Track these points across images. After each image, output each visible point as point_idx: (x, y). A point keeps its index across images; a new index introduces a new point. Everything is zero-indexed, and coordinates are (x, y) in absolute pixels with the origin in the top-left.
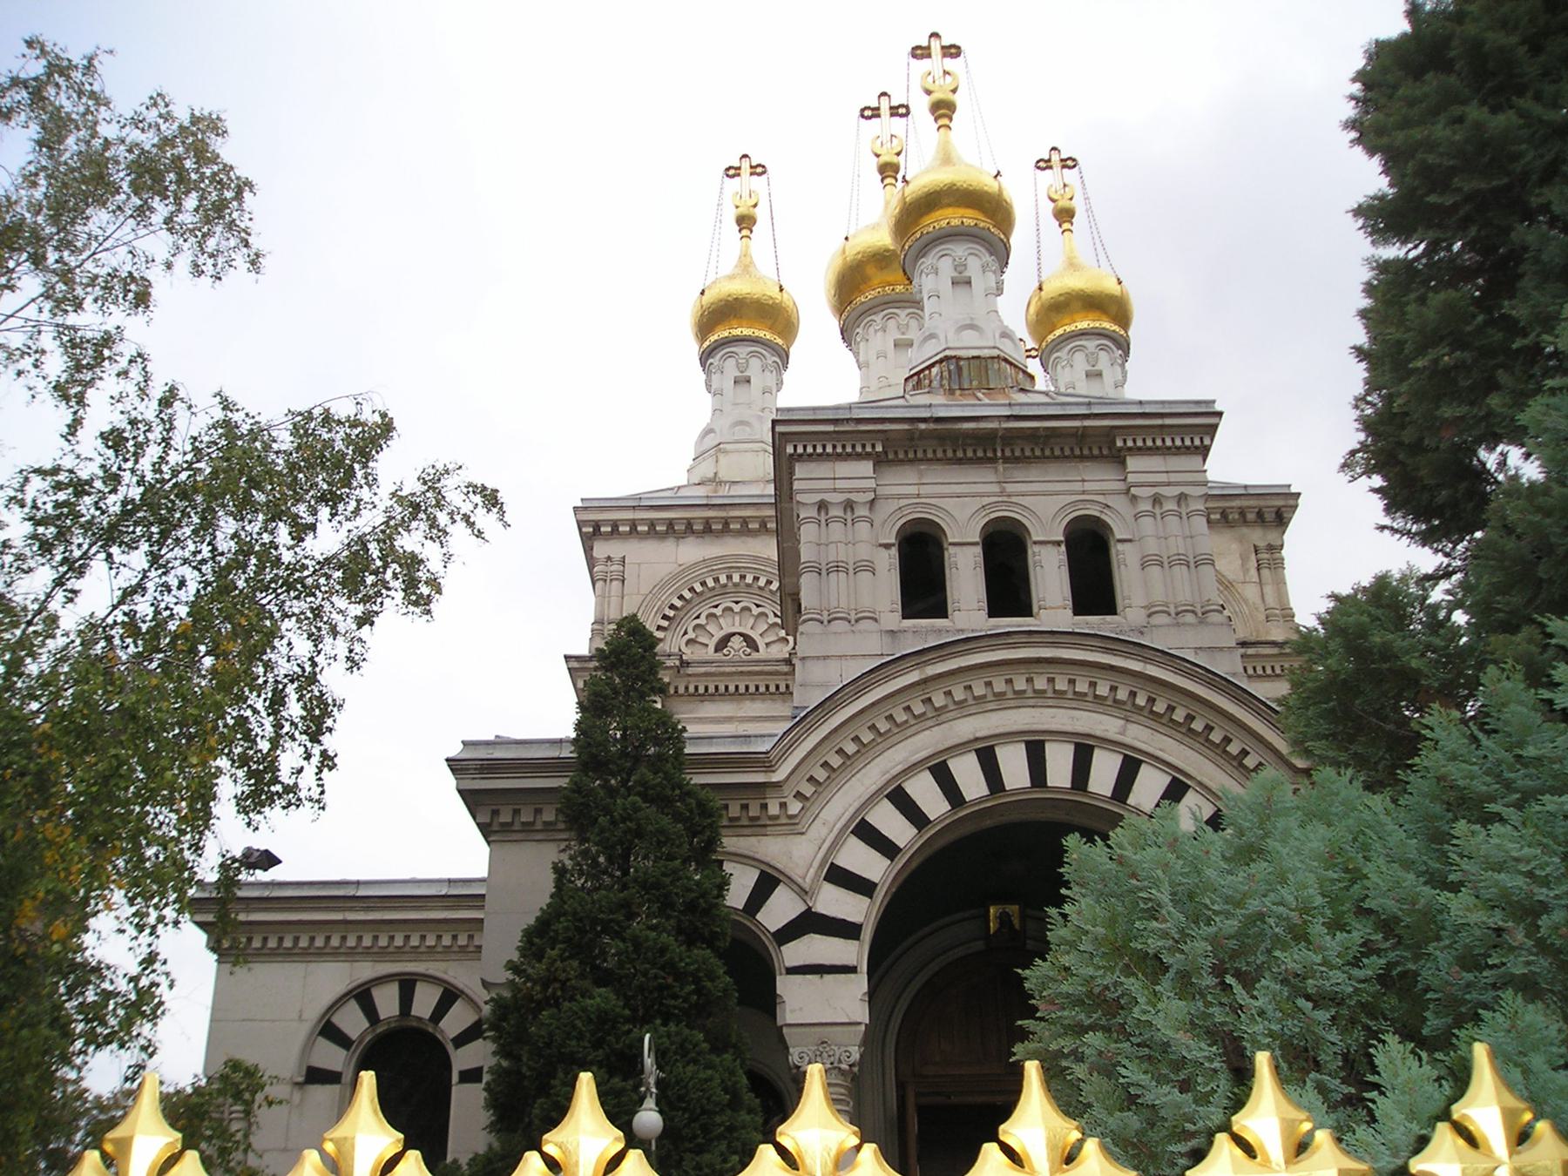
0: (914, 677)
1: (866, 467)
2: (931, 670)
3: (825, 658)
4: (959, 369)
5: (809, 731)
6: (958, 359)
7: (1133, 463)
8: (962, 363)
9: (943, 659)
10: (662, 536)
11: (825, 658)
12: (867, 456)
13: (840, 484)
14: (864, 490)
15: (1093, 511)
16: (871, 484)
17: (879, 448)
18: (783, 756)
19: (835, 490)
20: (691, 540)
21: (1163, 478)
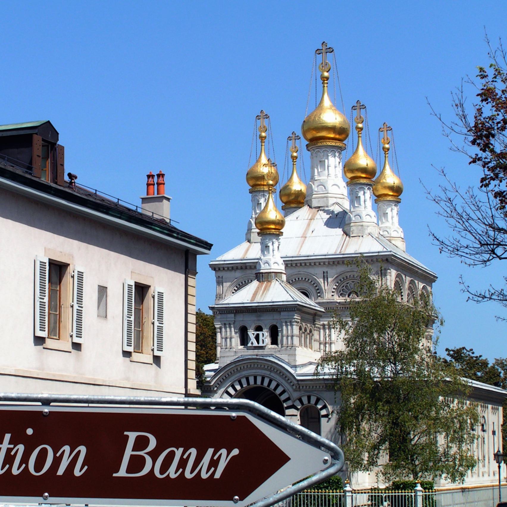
0: (234, 365)
1: (233, 315)
2: (237, 364)
3: (224, 357)
4: (263, 276)
5: (219, 374)
6: (262, 273)
7: (282, 313)
8: (263, 274)
9: (239, 362)
10: (231, 271)
11: (224, 357)
12: (233, 313)
13: (228, 319)
14: (232, 321)
15: (275, 324)
16: (234, 319)
17: (235, 312)
18: (212, 380)
19: (227, 321)
20: (238, 271)
21: (287, 317)
